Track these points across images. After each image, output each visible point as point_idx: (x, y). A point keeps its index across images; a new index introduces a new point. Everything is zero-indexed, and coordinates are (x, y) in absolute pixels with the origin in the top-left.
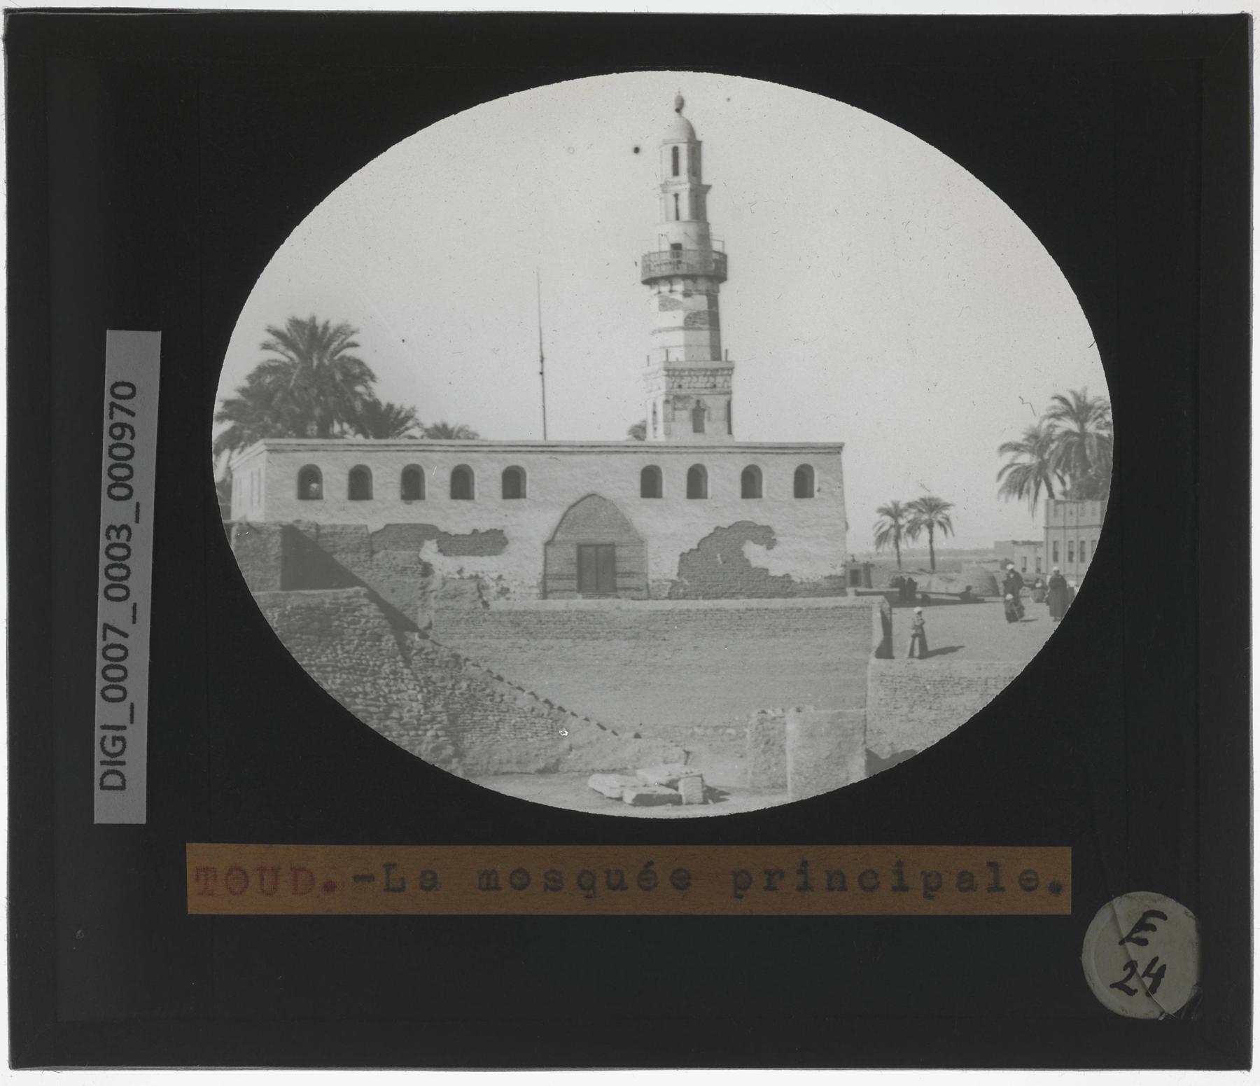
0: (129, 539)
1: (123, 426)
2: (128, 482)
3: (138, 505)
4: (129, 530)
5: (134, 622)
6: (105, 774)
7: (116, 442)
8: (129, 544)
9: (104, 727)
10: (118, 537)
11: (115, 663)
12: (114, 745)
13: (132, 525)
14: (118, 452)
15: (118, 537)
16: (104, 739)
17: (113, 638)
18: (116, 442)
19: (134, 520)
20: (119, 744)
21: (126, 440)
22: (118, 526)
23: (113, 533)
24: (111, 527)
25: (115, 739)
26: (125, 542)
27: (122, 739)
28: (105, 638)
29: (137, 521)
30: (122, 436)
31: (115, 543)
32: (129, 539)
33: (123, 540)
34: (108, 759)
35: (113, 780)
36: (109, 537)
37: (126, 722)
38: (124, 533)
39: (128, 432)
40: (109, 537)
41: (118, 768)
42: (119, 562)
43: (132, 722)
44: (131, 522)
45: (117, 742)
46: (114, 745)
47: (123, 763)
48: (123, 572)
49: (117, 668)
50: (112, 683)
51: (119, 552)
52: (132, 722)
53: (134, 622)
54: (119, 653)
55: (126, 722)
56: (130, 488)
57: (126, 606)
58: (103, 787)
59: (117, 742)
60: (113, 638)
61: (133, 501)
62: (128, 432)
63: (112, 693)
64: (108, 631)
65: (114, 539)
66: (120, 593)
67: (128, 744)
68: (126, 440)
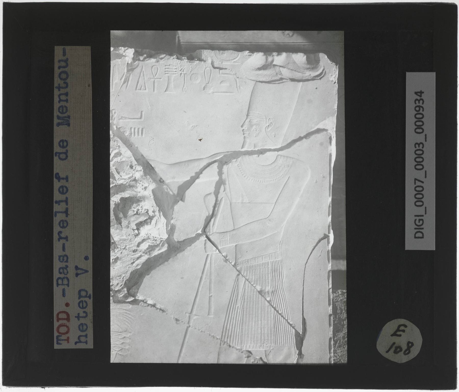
0: (423, 147)
1: (419, 107)
2: (422, 127)
3: (426, 135)
4: (423, 145)
5: (426, 177)
6: (416, 233)
7: (416, 112)
8: (423, 149)
9: (415, 216)
10: (419, 147)
11: (419, 193)
12: (419, 222)
13: (424, 142)
14: (418, 116)
15: (419, 147)
16: (415, 220)
17: (418, 183)
18: (416, 112)
19: (424, 140)
20: (421, 222)
21: (421, 111)
22: (419, 143)
23: (417, 146)
24: (416, 144)
25: (420, 220)
26: (422, 149)
27: (422, 220)
28: (415, 184)
29: (426, 141)
30: (420, 110)
31: (418, 149)
32: (423, 147)
33: (421, 148)
34: (418, 227)
35: (419, 235)
36: (416, 147)
37: (423, 214)
38: (421, 145)
39: (421, 109)
40: (416, 147)
41: (421, 230)
42: (419, 156)
43: (426, 213)
44: (423, 141)
45: (420, 221)
46: (419, 222)
47: (423, 229)
48: (421, 160)
49: (420, 194)
50: (420, 200)
51: (421, 152)
52: (426, 213)
53: (426, 177)
54: (421, 189)
55: (423, 214)
56: (423, 130)
57: (423, 171)
58: (415, 237)
59: (420, 221)
60: (418, 183)
61: (424, 134)
62: (421, 109)
63: (417, 204)
64: (416, 181)
65: (418, 148)
66: (421, 167)
67: (424, 222)
68: (421, 111)
